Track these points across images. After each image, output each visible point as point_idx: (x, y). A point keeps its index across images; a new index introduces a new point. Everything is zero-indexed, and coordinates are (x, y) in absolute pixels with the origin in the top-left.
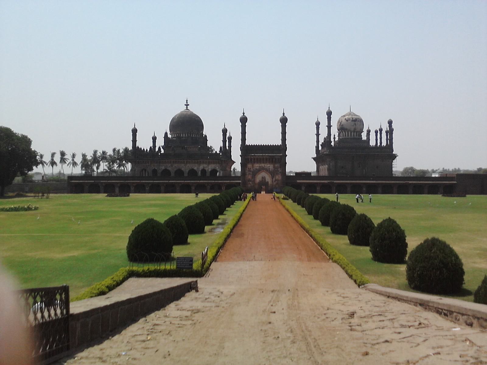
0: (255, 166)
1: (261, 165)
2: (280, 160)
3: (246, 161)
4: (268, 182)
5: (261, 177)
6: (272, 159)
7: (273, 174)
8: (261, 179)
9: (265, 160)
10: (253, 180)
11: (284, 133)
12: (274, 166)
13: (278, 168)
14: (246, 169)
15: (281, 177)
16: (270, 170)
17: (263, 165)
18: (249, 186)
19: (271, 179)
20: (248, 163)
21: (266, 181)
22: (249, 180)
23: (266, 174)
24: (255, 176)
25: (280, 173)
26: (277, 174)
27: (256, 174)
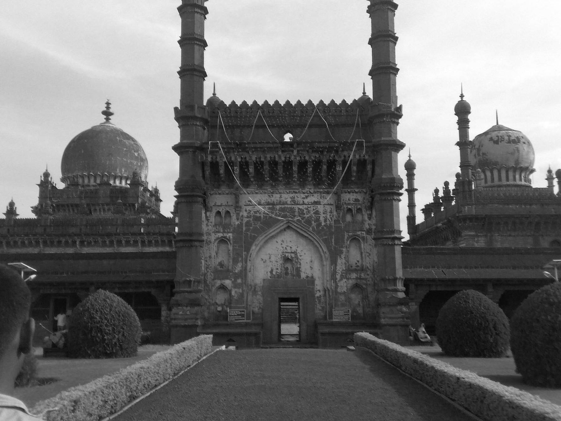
0: (250, 204)
1: (276, 197)
2: (369, 167)
3: (204, 177)
4: (311, 281)
5: (280, 252)
6: (332, 164)
7: (331, 240)
8: (276, 264)
9: (295, 168)
10: (238, 268)
11: (383, 40)
12: (339, 199)
13: (359, 210)
14: (207, 218)
15: (375, 251)
16: (318, 220)
17: (287, 197)
18: (221, 298)
19: (327, 263)
20: (218, 187)
21: (303, 276)
22: (222, 271)
23: (302, 241)
24: (248, 250)
25: (369, 232)
26: (355, 239)
27: (254, 238)
